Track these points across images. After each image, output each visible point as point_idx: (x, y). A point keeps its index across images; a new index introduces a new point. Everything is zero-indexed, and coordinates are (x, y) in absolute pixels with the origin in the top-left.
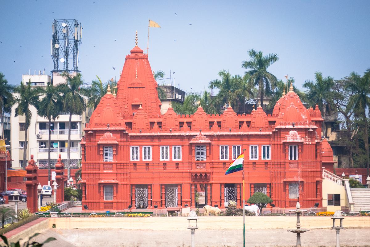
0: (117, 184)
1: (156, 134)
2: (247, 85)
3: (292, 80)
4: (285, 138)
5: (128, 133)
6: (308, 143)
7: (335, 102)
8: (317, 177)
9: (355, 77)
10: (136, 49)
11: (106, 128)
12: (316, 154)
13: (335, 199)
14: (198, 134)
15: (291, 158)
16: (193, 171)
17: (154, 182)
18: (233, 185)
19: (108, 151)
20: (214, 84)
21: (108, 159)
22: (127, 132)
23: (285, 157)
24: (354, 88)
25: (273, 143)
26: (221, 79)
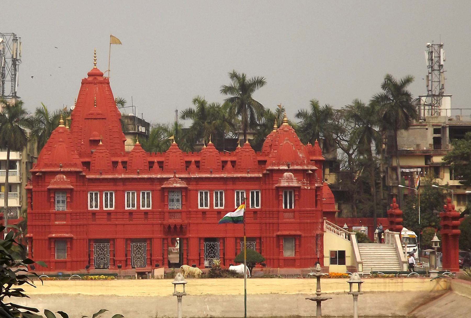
0: (71, 238)
1: (120, 177)
2: (227, 115)
3: (283, 109)
4: (278, 181)
5: (85, 176)
6: (306, 187)
7: (334, 136)
9: (359, 105)
10: (94, 71)
11: (59, 169)
13: (339, 257)
16: (165, 222)
18: (214, 240)
19: (60, 197)
21: (61, 207)
22: (84, 174)
23: (279, 204)
24: (357, 118)
25: (264, 187)
26: (195, 108)
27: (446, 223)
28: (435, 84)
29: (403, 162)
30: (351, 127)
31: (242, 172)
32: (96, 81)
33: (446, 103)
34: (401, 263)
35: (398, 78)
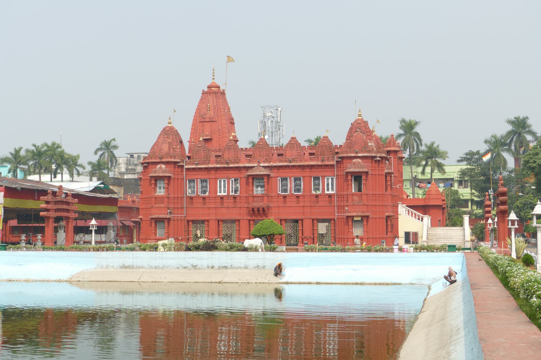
14: (255, 165)
16: (250, 206)
21: (161, 192)
22: (181, 164)
32: (214, 94)
34: (465, 241)
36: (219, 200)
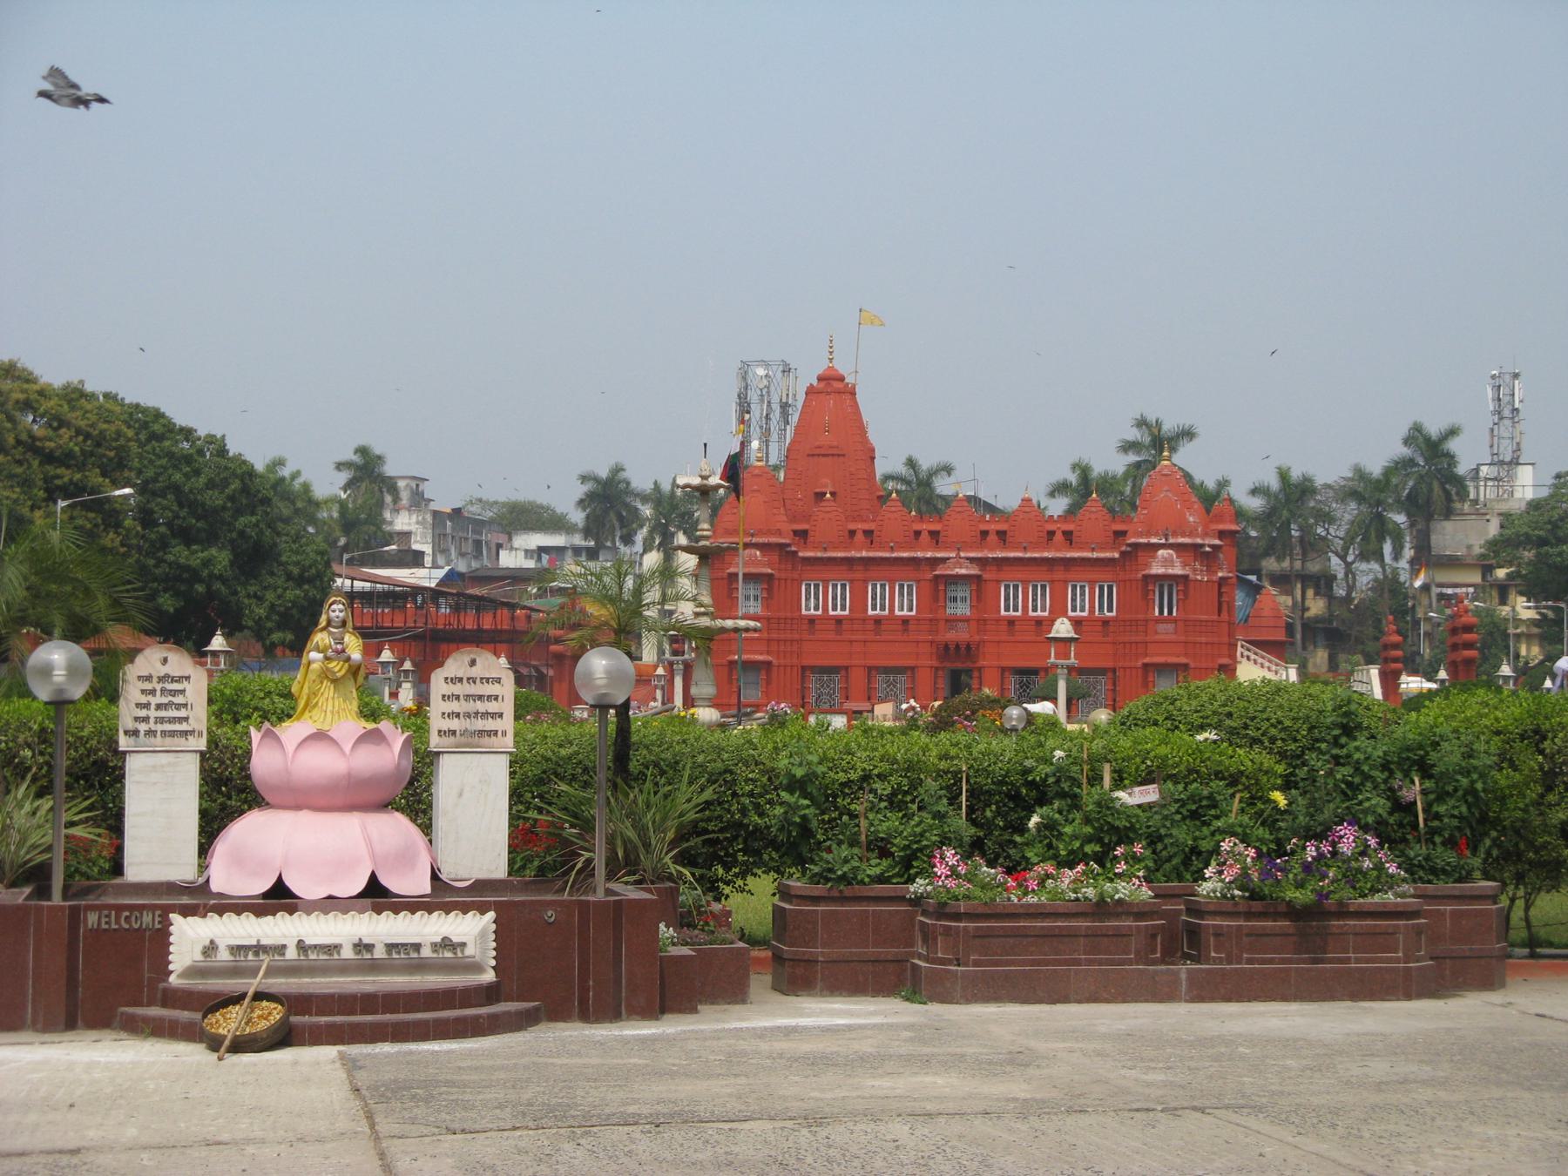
0: (769, 663)
2: (1128, 490)
4: (1148, 565)
5: (796, 553)
7: (1320, 530)
8: (1220, 656)
12: (1220, 604)
14: (953, 555)
15: (1161, 612)
16: (939, 638)
17: (855, 662)
18: (1035, 672)
20: (1060, 488)
26: (1073, 478)
27: (1456, 639)
28: (1505, 442)
29: (1442, 576)
30: (1348, 512)
31: (1081, 549)
33: (1525, 475)
35: (1434, 429)
36: (871, 626)
